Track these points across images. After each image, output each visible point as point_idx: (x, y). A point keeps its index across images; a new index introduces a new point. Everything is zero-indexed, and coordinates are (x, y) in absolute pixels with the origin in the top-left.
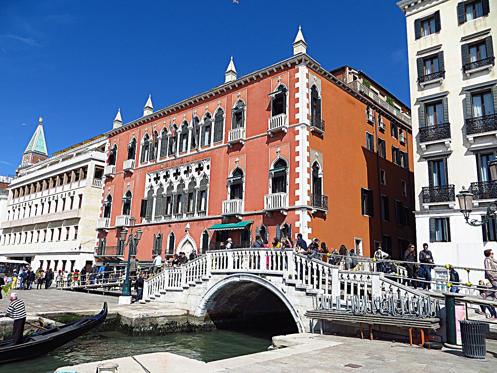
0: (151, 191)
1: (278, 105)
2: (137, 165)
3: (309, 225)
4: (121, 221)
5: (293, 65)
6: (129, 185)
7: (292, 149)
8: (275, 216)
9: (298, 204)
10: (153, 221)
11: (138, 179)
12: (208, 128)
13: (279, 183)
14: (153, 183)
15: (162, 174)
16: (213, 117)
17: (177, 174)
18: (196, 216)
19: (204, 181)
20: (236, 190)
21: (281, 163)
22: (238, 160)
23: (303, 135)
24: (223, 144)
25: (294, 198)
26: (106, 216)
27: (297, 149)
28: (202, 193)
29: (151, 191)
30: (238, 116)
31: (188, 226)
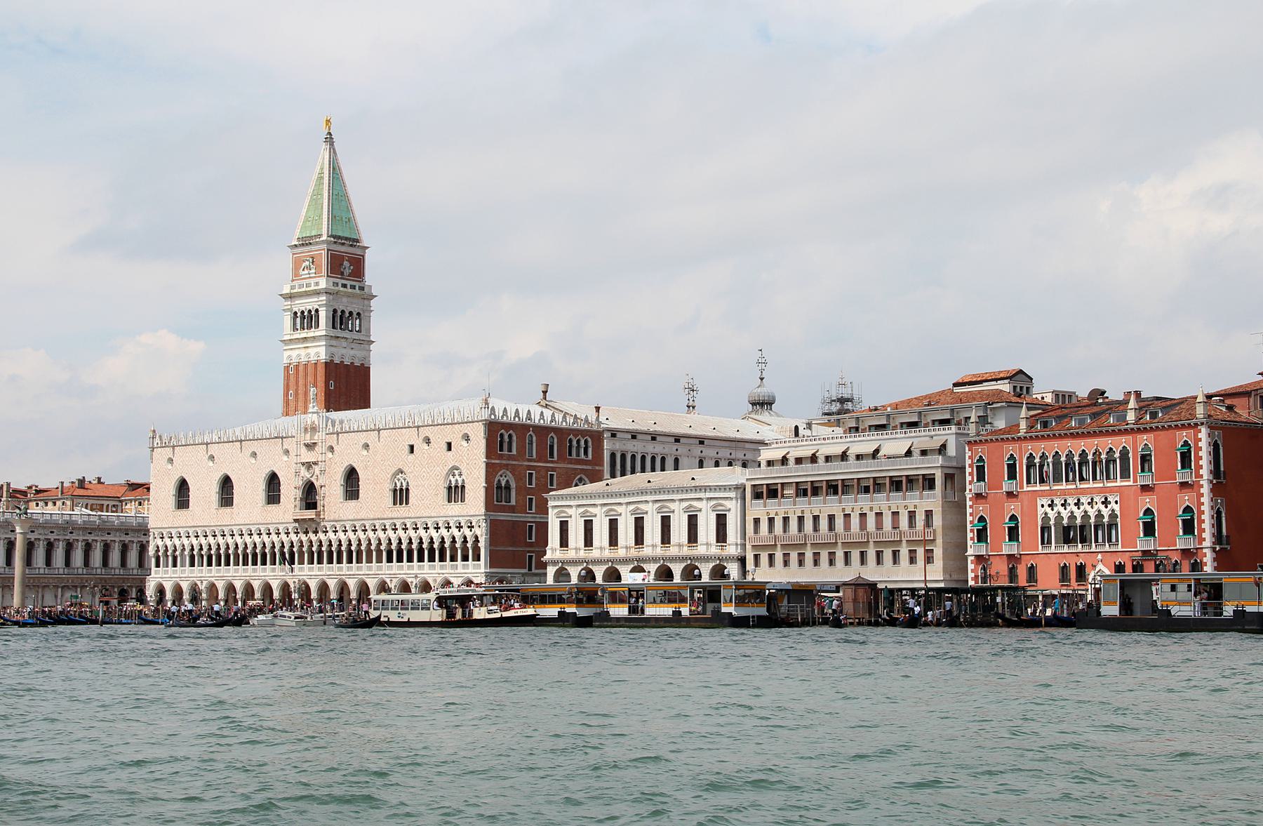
0: (1046, 518)
1: (1186, 460)
2: (1022, 487)
3: (1215, 560)
4: (1008, 548)
5: (1196, 425)
6: (1013, 507)
7: (1199, 500)
8: (1186, 553)
9: (1205, 544)
10: (1053, 550)
11: (1026, 503)
12: (1111, 460)
13: (1189, 527)
14: (1048, 510)
15: (1058, 501)
16: (1117, 455)
17: (1078, 504)
18: (1107, 548)
19: (1113, 515)
20: (1149, 529)
21: (1188, 510)
22: (1148, 501)
23: (1205, 490)
24: (1131, 483)
25: (1202, 540)
26: (979, 541)
27: (1202, 500)
28: (1113, 525)
29: (1046, 518)
30: (1145, 459)
31: (1100, 557)
